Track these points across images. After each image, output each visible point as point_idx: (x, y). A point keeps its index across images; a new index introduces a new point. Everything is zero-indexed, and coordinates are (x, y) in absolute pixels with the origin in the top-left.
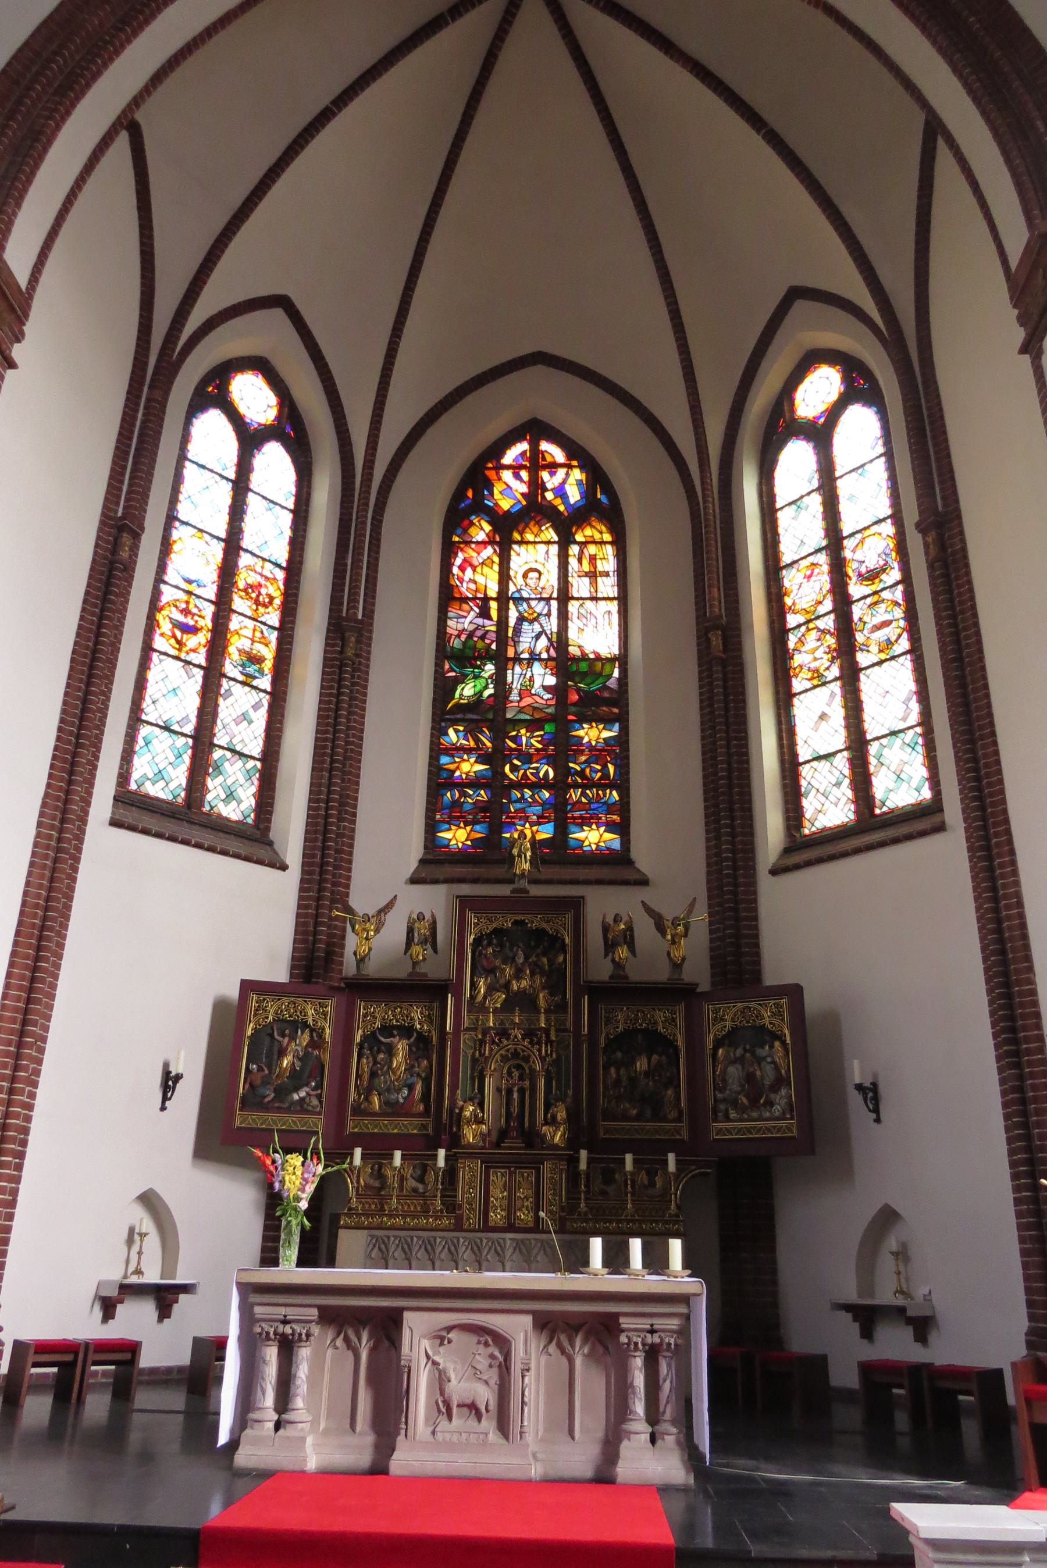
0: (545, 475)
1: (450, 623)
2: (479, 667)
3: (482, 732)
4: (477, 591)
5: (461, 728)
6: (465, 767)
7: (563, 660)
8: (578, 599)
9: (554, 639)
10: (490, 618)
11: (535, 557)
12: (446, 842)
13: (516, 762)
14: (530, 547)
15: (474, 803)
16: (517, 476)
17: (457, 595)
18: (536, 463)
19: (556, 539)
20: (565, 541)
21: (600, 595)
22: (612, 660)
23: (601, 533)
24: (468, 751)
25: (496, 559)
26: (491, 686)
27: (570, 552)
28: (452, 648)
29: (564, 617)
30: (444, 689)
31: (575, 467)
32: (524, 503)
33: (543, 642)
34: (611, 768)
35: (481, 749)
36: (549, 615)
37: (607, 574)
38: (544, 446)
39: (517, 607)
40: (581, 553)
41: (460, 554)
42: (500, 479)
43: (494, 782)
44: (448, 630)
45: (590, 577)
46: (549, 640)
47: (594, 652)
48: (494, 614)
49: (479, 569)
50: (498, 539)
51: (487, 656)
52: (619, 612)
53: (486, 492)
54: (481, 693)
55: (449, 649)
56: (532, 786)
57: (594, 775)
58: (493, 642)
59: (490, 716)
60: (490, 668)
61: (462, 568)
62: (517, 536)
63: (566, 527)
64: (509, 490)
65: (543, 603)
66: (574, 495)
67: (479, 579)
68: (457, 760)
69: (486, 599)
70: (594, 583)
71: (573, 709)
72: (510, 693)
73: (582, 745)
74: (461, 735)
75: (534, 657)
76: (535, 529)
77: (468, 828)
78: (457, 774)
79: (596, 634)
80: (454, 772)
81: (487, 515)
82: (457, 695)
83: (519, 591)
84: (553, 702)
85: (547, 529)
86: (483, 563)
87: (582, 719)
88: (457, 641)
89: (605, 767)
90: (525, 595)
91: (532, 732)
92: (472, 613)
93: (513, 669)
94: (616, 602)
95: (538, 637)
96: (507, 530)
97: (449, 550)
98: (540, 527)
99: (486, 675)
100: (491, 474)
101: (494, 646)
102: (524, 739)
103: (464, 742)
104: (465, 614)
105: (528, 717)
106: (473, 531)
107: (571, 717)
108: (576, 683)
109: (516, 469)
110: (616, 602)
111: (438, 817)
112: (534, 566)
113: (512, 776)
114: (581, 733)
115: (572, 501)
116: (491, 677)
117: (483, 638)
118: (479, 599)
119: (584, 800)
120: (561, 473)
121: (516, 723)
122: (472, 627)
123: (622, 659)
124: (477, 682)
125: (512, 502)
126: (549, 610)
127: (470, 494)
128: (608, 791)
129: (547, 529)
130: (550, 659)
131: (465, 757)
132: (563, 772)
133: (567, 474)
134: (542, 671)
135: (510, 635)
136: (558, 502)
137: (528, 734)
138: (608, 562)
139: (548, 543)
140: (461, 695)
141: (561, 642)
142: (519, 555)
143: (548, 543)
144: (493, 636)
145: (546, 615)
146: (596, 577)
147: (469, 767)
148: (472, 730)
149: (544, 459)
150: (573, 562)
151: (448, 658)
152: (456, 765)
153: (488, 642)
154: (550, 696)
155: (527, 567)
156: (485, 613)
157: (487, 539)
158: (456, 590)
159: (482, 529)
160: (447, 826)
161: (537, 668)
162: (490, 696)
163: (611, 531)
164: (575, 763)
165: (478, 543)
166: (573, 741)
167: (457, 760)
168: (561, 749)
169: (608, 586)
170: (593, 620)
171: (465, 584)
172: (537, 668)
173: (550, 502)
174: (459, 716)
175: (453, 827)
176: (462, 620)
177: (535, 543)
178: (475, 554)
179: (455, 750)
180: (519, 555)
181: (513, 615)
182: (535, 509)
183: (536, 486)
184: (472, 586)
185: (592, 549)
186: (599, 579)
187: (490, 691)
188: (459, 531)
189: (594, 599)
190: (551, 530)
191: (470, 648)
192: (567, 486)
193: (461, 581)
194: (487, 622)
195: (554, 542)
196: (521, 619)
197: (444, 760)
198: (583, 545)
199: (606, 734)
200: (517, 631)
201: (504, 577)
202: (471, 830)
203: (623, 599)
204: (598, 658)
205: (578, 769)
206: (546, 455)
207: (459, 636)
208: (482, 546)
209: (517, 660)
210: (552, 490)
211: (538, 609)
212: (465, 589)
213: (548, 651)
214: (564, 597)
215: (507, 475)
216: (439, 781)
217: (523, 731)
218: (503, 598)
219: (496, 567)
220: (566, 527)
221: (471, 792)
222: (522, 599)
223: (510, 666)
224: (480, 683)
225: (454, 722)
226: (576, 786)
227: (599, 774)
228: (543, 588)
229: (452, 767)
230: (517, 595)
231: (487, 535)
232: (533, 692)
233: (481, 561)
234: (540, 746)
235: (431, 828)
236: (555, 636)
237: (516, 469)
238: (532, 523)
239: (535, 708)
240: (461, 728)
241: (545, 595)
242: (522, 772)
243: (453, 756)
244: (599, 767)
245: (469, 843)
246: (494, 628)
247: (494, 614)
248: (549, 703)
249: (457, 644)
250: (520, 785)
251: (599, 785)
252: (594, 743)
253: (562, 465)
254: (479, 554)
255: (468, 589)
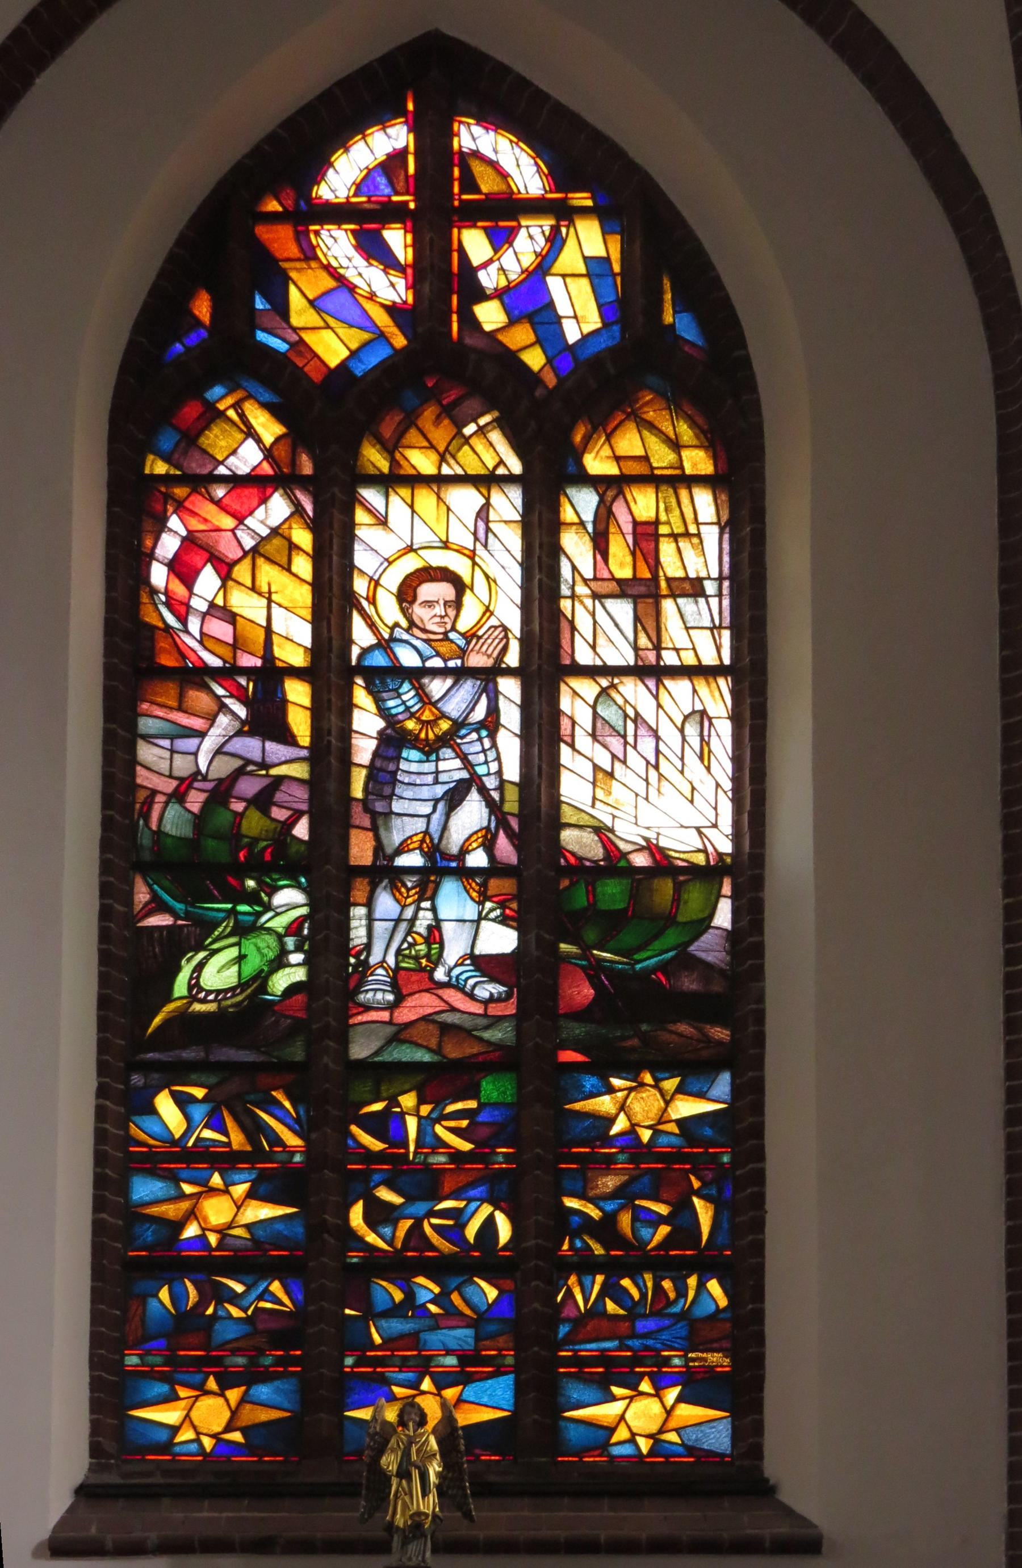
0: (475, 243)
1: (146, 752)
2: (252, 898)
3: (271, 1105)
4: (237, 645)
5: (199, 1093)
6: (217, 1211)
7: (541, 868)
8: (591, 672)
9: (511, 806)
10: (287, 738)
11: (442, 532)
12: (163, 1436)
13: (385, 1194)
14: (425, 499)
15: (248, 1320)
16: (373, 248)
17: (168, 661)
18: (438, 198)
19: (516, 467)
20: (546, 481)
21: (670, 659)
22: (709, 873)
23: (676, 445)
24: (226, 1161)
25: (303, 537)
26: (296, 958)
27: (568, 514)
28: (159, 833)
29: (543, 733)
30: (133, 968)
31: (584, 211)
32: (400, 341)
33: (472, 815)
34: (704, 1213)
35: (268, 1157)
36: (492, 724)
37: (694, 588)
38: (473, 137)
39: (378, 701)
40: (604, 516)
41: (174, 522)
42: (309, 254)
43: (311, 1255)
44: (143, 778)
45: (636, 599)
46: (494, 807)
47: (651, 848)
48: (300, 722)
49: (242, 572)
50: (307, 467)
51: (281, 861)
52: (736, 717)
53: (260, 304)
54: (261, 979)
55: (146, 840)
56: (440, 1268)
57: (645, 1232)
58: (297, 815)
59: (297, 1052)
60: (290, 900)
61: (183, 569)
62: (375, 458)
63: (552, 425)
64: (344, 295)
65: (468, 688)
66: (578, 311)
67: (246, 604)
68: (188, 1189)
69: (272, 675)
70: (647, 619)
71: (578, 1030)
72: (362, 981)
73: (608, 1140)
74: (199, 1112)
75: (441, 865)
76: (441, 435)
77: (234, 1395)
78: (191, 1231)
79: (658, 791)
80: (180, 1225)
81: (268, 383)
82: (180, 987)
83: (385, 645)
84: (510, 1008)
85: (482, 431)
86: (255, 552)
87: (609, 1062)
88: (173, 811)
89: (682, 1210)
90: (408, 658)
91: (439, 1102)
92: (223, 720)
93: (369, 904)
94: (724, 684)
95: (454, 798)
96: (339, 439)
97: (132, 512)
98: (460, 426)
99: (279, 923)
100: (280, 240)
101: (301, 830)
102: (412, 1124)
103: (208, 1134)
104: (197, 723)
105: (427, 1057)
106: (217, 440)
107: (569, 1056)
108: (586, 950)
109: (366, 220)
110: (724, 684)
111: (132, 1360)
112: (438, 559)
113: (371, 1238)
114: (605, 1104)
115: (572, 334)
116: (294, 928)
117: (263, 801)
118: (249, 672)
119: (611, 1307)
120: (530, 238)
121: (383, 1075)
122: (224, 767)
123: (745, 869)
124: (249, 946)
125: (356, 338)
126: (493, 711)
127: (203, 308)
128: (692, 1281)
129: (482, 431)
130: (496, 869)
131: (216, 1180)
132: (543, 1221)
133: (555, 241)
134: (471, 911)
135: (357, 791)
136: (521, 336)
137: (425, 1110)
138: (701, 553)
139: (486, 481)
140: (195, 985)
141: (534, 810)
142: (383, 522)
143: (486, 481)
144: (300, 795)
145: (482, 725)
146: (657, 598)
147: (228, 1211)
148: (235, 1096)
149: (470, 183)
150: (576, 548)
151: (145, 869)
152: (185, 1205)
153: (279, 814)
154: (496, 989)
155: (411, 564)
156: (267, 720)
157: (267, 469)
158: (163, 644)
159: (250, 433)
160: (162, 1388)
161: (454, 902)
162: (292, 989)
163: (711, 440)
164: (582, 1196)
165: (235, 481)
166: (578, 1128)
167: (188, 1189)
168: (540, 1150)
169: (694, 629)
170: (647, 746)
171: (194, 625)
172: (454, 902)
173: (492, 334)
174: (189, 1054)
175: (183, 1393)
176: (191, 743)
177: (438, 481)
178: (228, 522)
179: (177, 1160)
180: (383, 522)
181: (366, 723)
182: (438, 365)
183: (441, 280)
184: (222, 630)
185: (644, 503)
186: (668, 606)
187: (291, 975)
188: (167, 440)
189: (651, 672)
190: (496, 436)
191: (218, 836)
192: (554, 284)
193: (182, 610)
194: (276, 750)
195: (511, 479)
196: (393, 740)
197: (145, 1189)
198: (613, 488)
199: (687, 1108)
200: (383, 777)
201: (334, 598)
202: (243, 1400)
203: (749, 674)
204: (663, 863)
205: (595, 1213)
206: (478, 168)
207: (179, 796)
208: (252, 493)
209: (384, 872)
210: (499, 294)
211: (454, 707)
212: (197, 639)
213: (489, 845)
214: (546, 662)
215: (337, 244)
216: (130, 1254)
217: (408, 1101)
218: (331, 669)
219: (303, 566)
220: (552, 425)
221: (239, 1288)
222: (399, 672)
223: (359, 893)
224: (258, 951)
225: (173, 1075)
226: (587, 1266)
227: (664, 1230)
228: (470, 636)
229: (171, 1211)
230: (379, 659)
231: (269, 453)
232: (440, 975)
233: (249, 543)
234: (466, 1146)
235: (111, 1395)
236: (512, 795)
237: (366, 220)
238: (429, 413)
239: (446, 1029)
240: (199, 1093)
241: (476, 660)
242: (405, 1225)
243: (175, 1179)
244: (663, 1209)
245: (237, 1436)
246: (300, 771)
247: (300, 722)
248: (494, 1010)
249: (173, 821)
250: (400, 1266)
251: (661, 1263)
252: (646, 1135)
253: (535, 207)
254: (240, 519)
255: (204, 638)
